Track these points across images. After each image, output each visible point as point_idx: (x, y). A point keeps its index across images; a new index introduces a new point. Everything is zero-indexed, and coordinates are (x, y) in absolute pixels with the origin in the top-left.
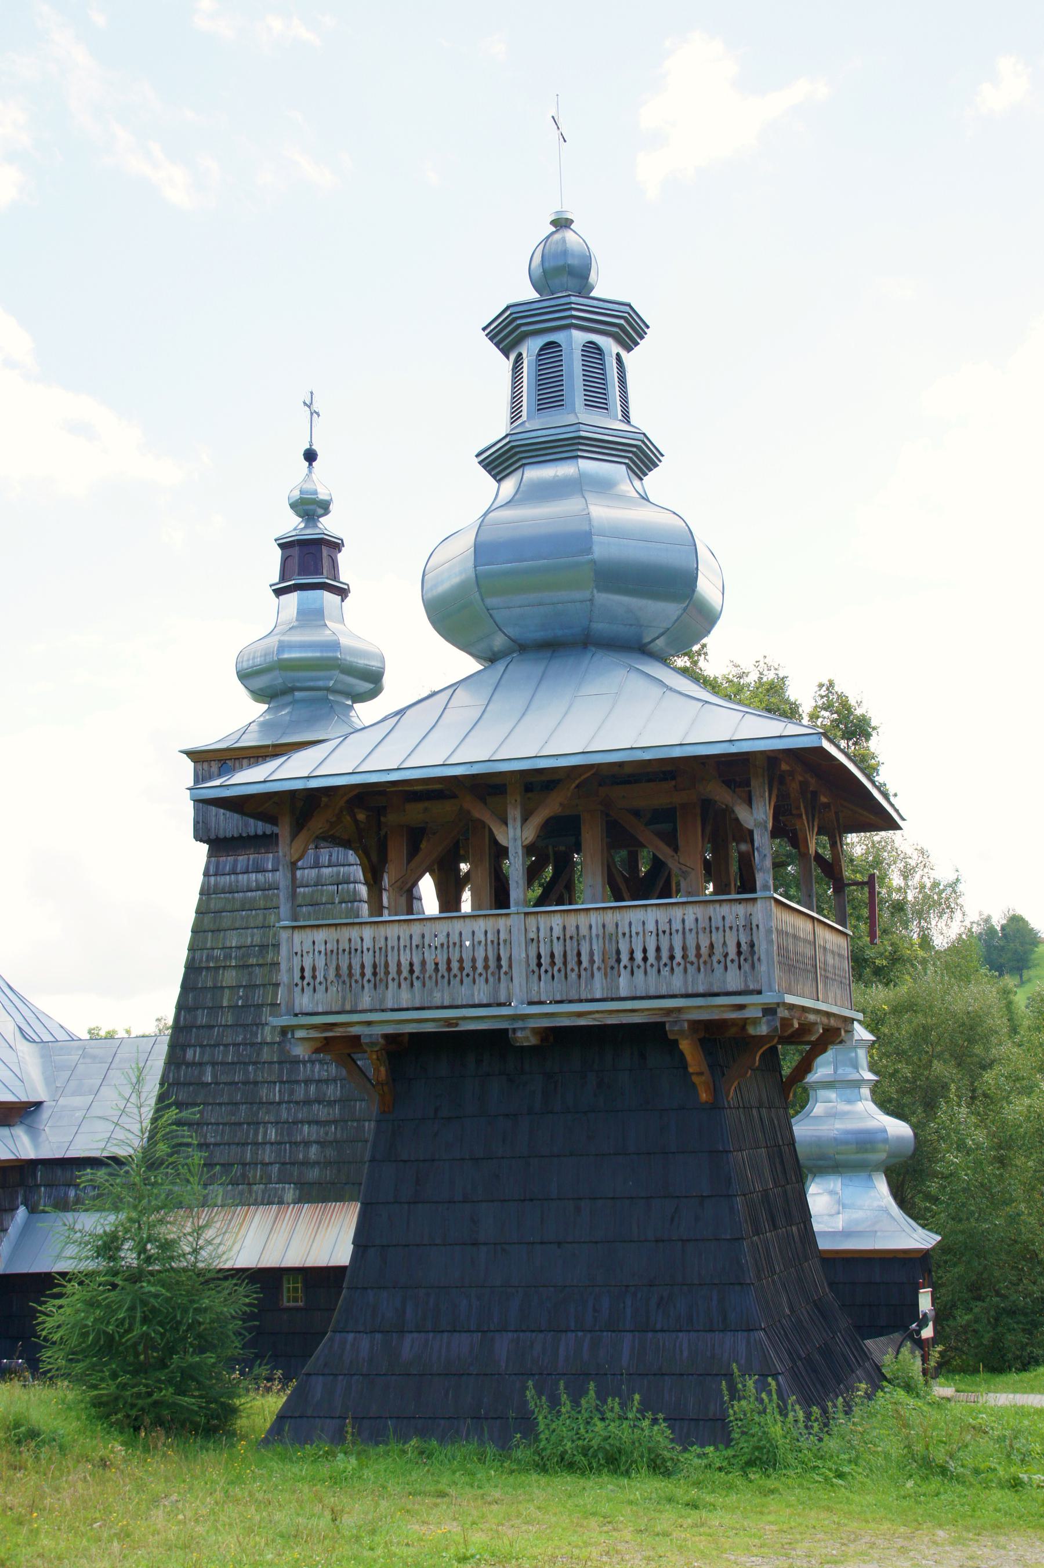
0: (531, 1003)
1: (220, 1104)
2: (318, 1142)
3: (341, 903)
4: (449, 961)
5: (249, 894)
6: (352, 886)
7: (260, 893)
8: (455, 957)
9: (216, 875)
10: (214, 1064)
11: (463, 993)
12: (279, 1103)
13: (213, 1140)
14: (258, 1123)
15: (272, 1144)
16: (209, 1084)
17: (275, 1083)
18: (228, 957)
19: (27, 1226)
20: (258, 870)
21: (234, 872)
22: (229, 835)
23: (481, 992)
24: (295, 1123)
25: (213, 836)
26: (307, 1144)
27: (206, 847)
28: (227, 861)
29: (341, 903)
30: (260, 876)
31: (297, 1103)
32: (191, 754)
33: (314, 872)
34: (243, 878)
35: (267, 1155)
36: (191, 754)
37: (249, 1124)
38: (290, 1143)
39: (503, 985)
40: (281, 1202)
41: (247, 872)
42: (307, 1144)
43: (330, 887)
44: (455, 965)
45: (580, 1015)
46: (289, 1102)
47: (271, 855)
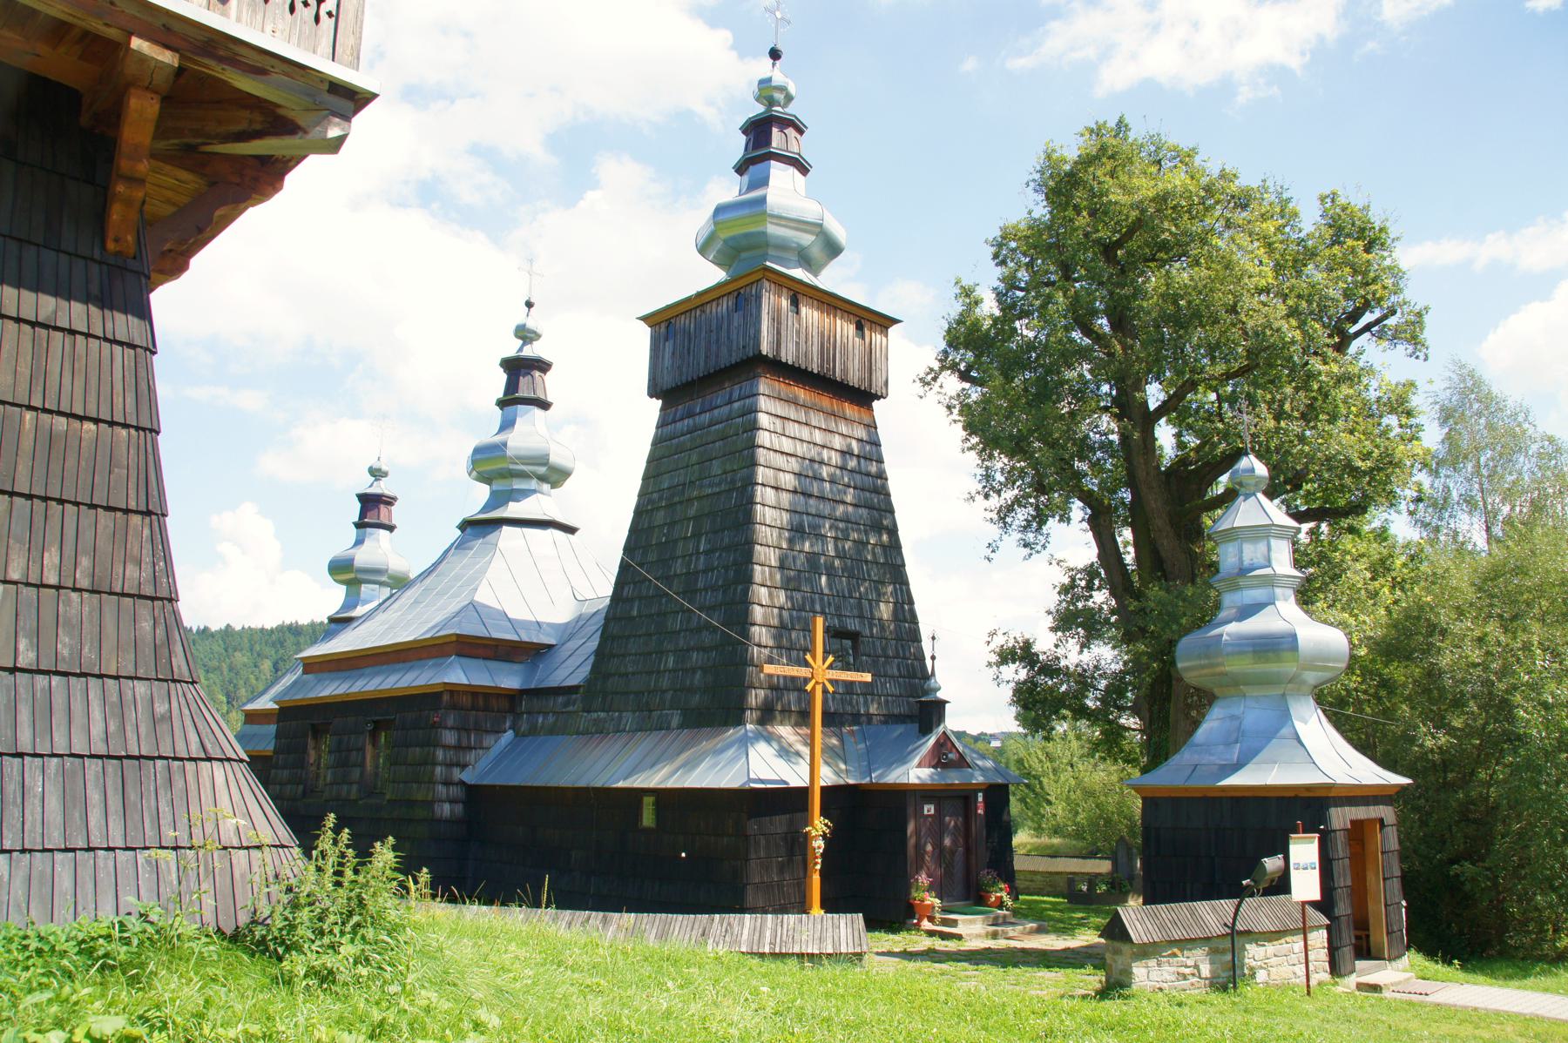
1: (640, 636)
2: (701, 668)
3: (743, 433)
5: (682, 438)
7: (689, 436)
10: (640, 598)
12: (679, 632)
13: (630, 670)
14: (662, 653)
15: (670, 671)
16: (634, 618)
17: (678, 613)
18: (661, 498)
19: (512, 745)
22: (669, 387)
24: (688, 650)
25: (662, 391)
26: (694, 670)
27: (657, 404)
30: (691, 421)
31: (692, 631)
32: (645, 319)
34: (679, 425)
35: (665, 682)
36: (645, 319)
37: (657, 653)
38: (682, 670)
40: (668, 728)
42: (694, 670)
46: (687, 630)
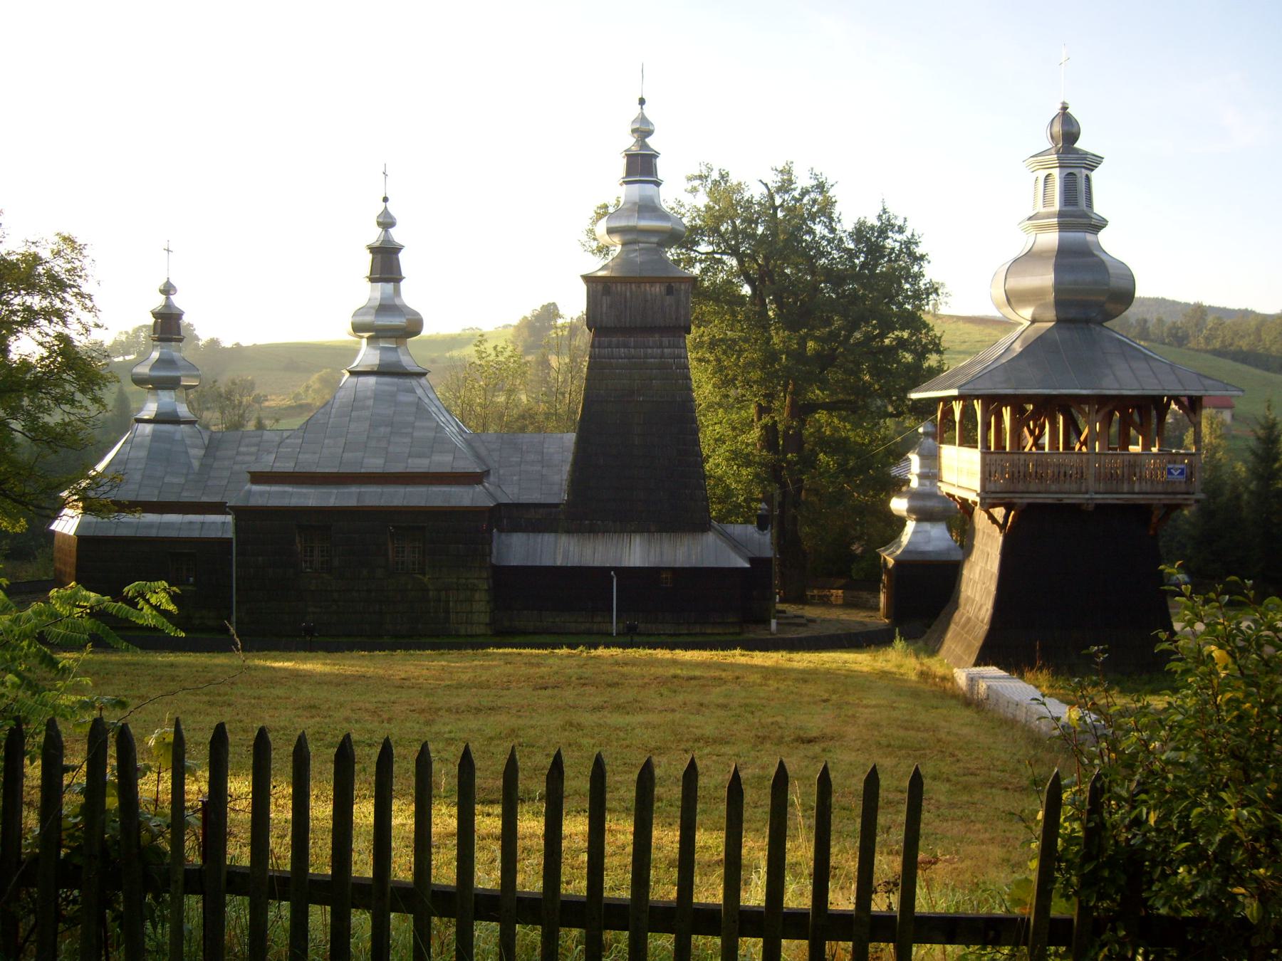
0: (1096, 493)
3: (676, 369)
4: (1059, 473)
6: (682, 360)
8: (1062, 471)
9: (599, 347)
11: (1067, 486)
20: (626, 346)
21: (609, 346)
23: (1074, 487)
28: (605, 340)
29: (676, 369)
30: (626, 350)
33: (659, 351)
39: (1084, 484)
40: (649, 531)
41: (618, 347)
43: (669, 360)
44: (1062, 474)
45: (1118, 499)
47: (632, 339)
